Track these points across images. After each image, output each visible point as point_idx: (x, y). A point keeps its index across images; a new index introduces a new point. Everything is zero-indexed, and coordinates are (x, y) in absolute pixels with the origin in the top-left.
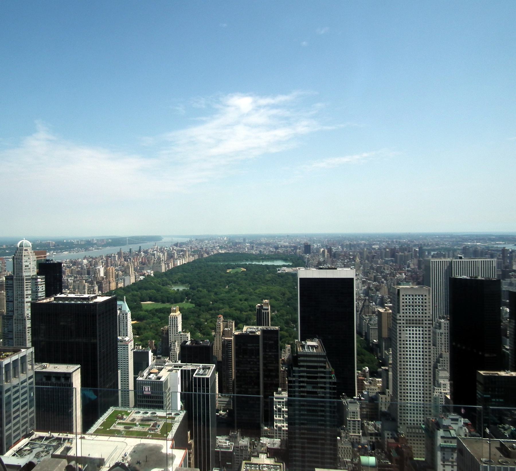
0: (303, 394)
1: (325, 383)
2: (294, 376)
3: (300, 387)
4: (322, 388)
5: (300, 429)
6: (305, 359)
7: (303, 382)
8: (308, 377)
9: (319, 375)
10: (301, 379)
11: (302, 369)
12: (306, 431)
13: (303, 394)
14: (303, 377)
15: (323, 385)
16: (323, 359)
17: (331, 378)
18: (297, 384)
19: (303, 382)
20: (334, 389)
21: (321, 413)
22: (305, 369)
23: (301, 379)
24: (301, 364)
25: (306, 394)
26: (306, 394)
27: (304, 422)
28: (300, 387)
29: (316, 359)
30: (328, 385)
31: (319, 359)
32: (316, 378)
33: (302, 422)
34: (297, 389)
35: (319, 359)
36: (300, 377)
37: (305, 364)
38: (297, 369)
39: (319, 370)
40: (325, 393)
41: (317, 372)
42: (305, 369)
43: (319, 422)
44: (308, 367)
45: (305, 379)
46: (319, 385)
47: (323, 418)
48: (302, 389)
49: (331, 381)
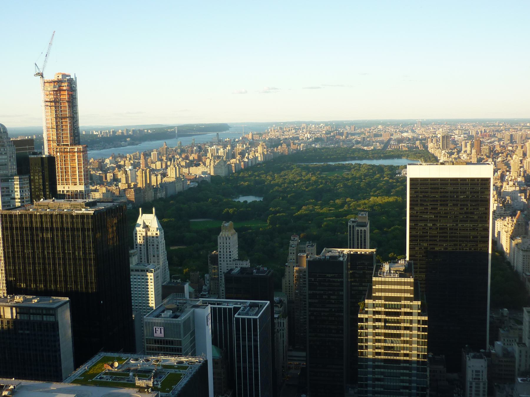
0: (379, 338)
1: (411, 322)
2: (367, 312)
3: (375, 327)
4: (406, 328)
5: (374, 386)
6: (383, 287)
7: (379, 320)
8: (387, 314)
9: (403, 310)
10: (377, 316)
11: (377, 302)
12: (382, 389)
13: (379, 338)
14: (379, 313)
15: (408, 325)
16: (409, 288)
17: (419, 314)
18: (370, 323)
19: (379, 320)
20: (424, 330)
21: (405, 365)
22: (383, 302)
23: (377, 316)
24: (377, 294)
25: (383, 338)
26: (383, 338)
27: (379, 376)
28: (375, 327)
29: (399, 287)
30: (415, 325)
31: (403, 287)
32: (398, 314)
33: (376, 376)
34: (370, 330)
35: (403, 287)
36: (375, 313)
37: (383, 294)
38: (371, 301)
39: (403, 302)
40: (411, 336)
41: (400, 307)
42: (383, 302)
43: (402, 378)
44: (387, 299)
45: (383, 317)
46: (402, 325)
47: (408, 371)
48: (377, 331)
49: (419, 318)
